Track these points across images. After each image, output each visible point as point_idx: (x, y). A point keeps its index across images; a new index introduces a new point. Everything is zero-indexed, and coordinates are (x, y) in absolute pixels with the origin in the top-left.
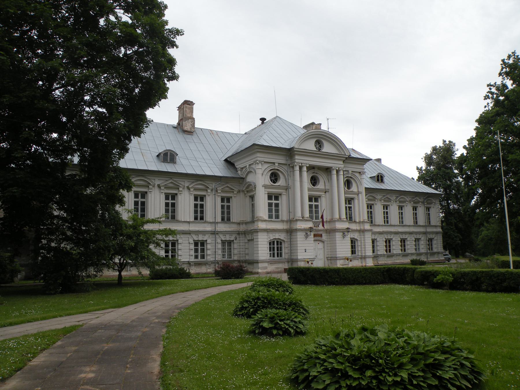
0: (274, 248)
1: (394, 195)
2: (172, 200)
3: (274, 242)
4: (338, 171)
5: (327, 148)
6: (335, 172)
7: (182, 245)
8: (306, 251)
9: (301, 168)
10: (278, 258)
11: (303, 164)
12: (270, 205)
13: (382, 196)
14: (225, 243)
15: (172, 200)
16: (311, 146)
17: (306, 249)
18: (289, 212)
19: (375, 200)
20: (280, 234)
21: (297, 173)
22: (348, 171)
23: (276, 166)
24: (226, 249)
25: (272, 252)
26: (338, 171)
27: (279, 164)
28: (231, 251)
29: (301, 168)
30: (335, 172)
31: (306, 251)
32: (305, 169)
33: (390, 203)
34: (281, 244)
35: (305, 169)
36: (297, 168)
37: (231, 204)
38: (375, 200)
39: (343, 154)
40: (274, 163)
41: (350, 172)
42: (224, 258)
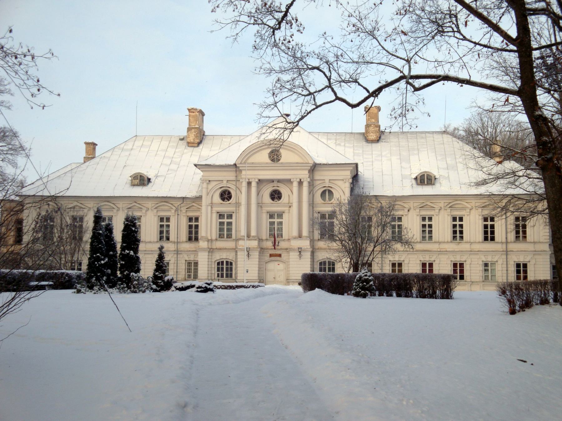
0: (222, 268)
1: (442, 202)
2: (166, 222)
3: (222, 262)
4: (300, 183)
5: (286, 156)
7: (146, 265)
8: (247, 272)
9: (249, 184)
10: (227, 279)
11: (250, 181)
12: (221, 224)
13: (420, 204)
14: (192, 263)
15: (166, 222)
16: (263, 157)
17: (247, 270)
18: (236, 231)
19: (404, 210)
20: (228, 254)
21: (244, 189)
22: (324, 180)
23: (224, 184)
24: (193, 269)
25: (220, 273)
26: (300, 183)
27: (228, 181)
28: (188, 270)
29: (249, 184)
30: (295, 184)
31: (247, 272)
32: (254, 184)
34: (231, 264)
35: (254, 184)
36: (244, 184)
37: (199, 224)
38: (404, 210)
39: (307, 162)
40: (222, 181)
41: (327, 181)
42: (190, 278)
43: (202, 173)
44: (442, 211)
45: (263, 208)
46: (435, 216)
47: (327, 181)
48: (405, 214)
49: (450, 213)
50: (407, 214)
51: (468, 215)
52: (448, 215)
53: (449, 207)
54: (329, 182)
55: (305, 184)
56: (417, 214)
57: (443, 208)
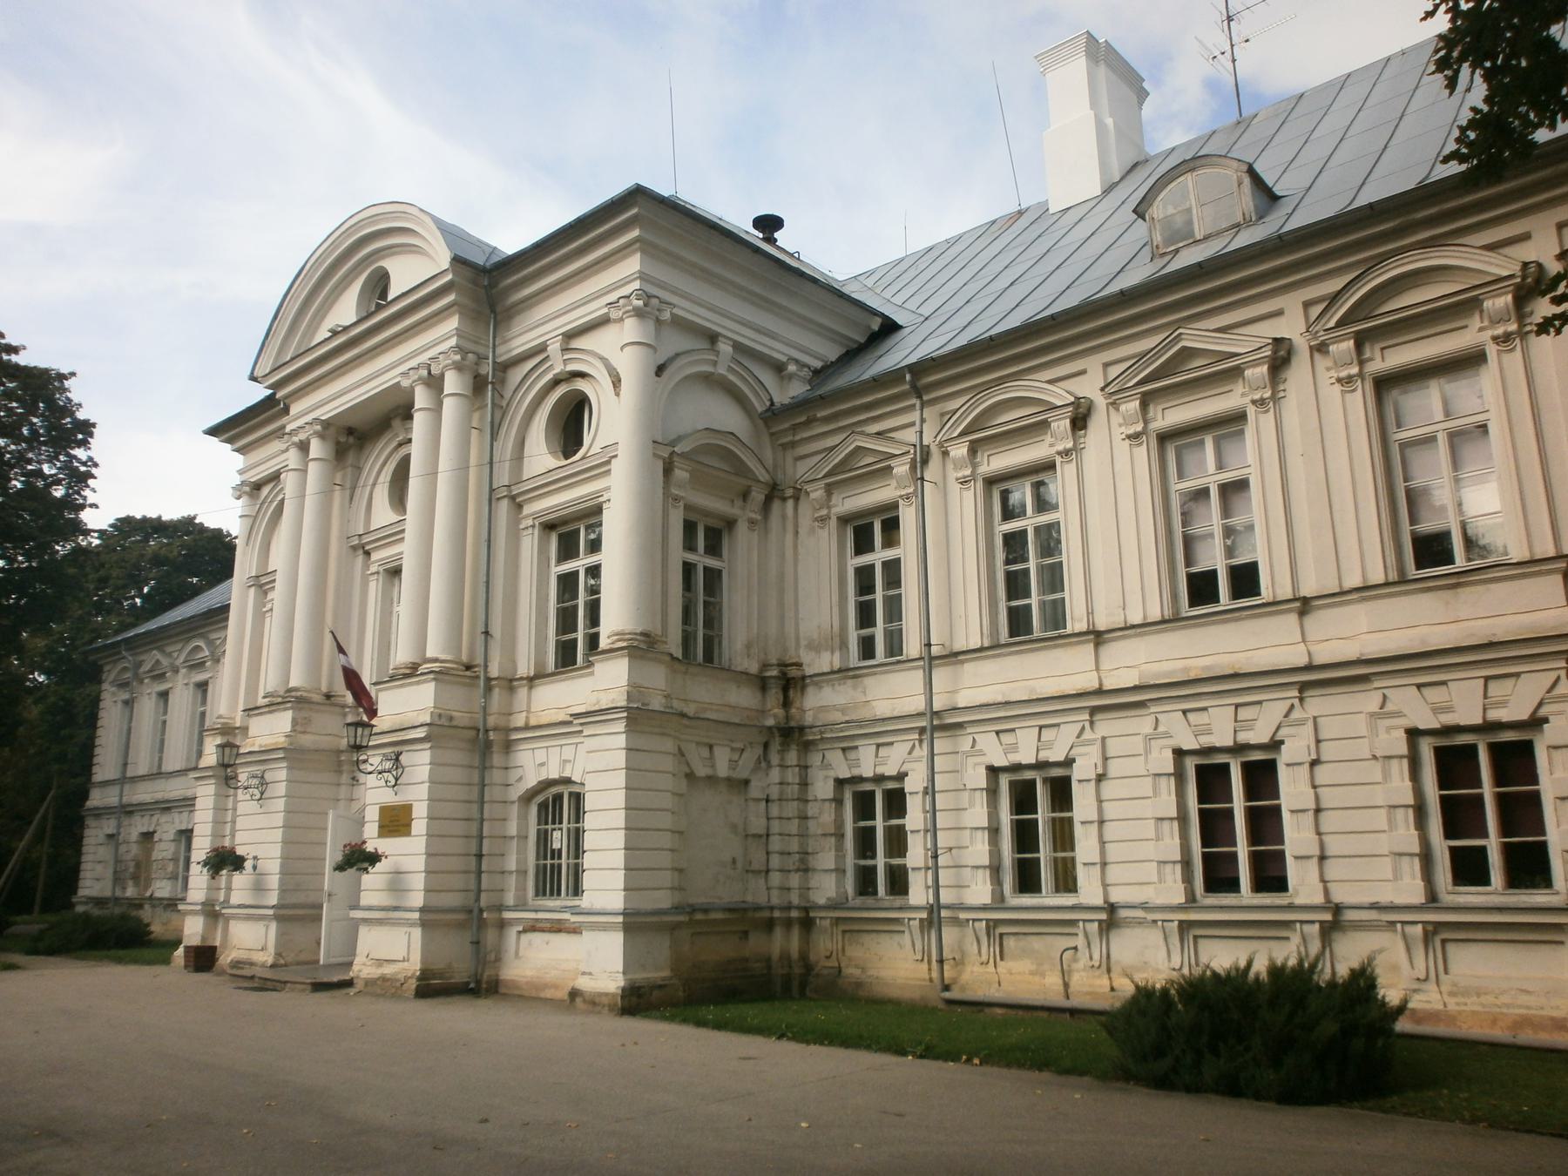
1: (1292, 303)
4: (435, 383)
6: (421, 398)
11: (302, 436)
32: (316, 449)
33: (1239, 388)
43: (239, 460)
44: (1298, 374)
45: (375, 556)
46: (1251, 411)
47: (554, 347)
48: (1060, 448)
49: (1361, 363)
50: (1070, 445)
51: (1506, 338)
52: (1346, 381)
53: (1341, 323)
54: (565, 350)
55: (452, 383)
56: (1131, 431)
57: (1301, 344)
